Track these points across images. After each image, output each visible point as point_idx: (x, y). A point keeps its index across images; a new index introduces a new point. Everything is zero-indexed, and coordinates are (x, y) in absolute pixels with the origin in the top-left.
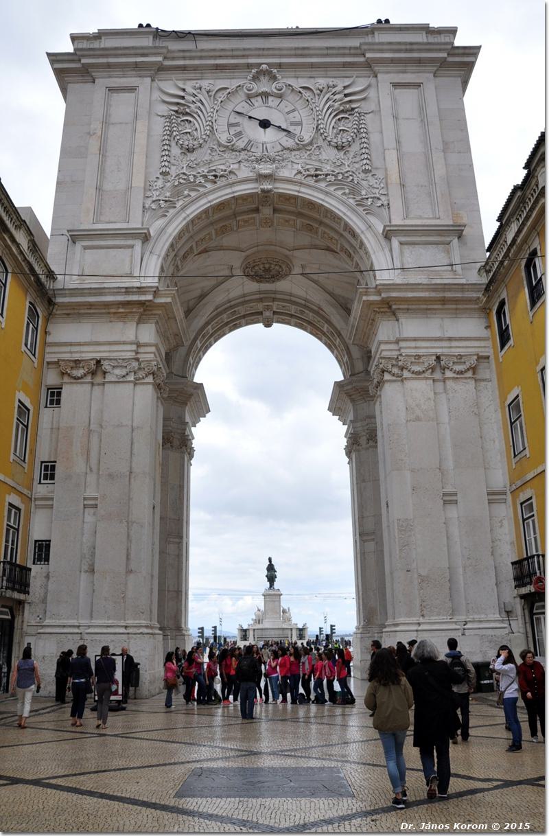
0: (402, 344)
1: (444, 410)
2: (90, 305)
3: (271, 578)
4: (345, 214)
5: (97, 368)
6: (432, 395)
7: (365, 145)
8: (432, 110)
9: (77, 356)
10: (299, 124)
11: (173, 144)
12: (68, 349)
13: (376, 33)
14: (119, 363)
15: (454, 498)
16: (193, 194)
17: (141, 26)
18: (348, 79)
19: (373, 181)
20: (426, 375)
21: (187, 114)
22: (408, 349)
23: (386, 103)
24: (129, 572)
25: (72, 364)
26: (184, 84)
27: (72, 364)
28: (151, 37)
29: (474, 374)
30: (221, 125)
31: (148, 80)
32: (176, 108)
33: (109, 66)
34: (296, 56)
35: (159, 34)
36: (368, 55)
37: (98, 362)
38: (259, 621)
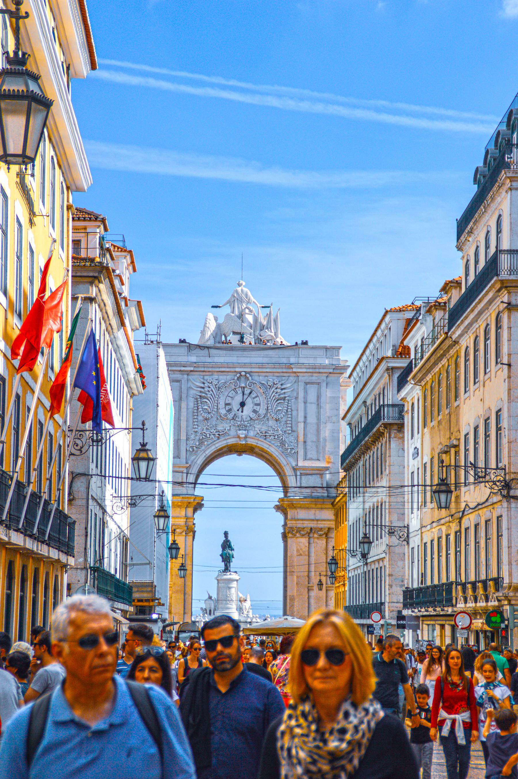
0: (298, 522)
1: (313, 550)
3: (227, 559)
6: (307, 545)
7: (289, 419)
10: (259, 405)
13: (300, 349)
17: (180, 340)
18: (283, 378)
19: (292, 439)
20: (306, 536)
22: (300, 524)
23: (301, 395)
28: (186, 348)
29: (326, 536)
30: (222, 405)
31: (186, 376)
34: (259, 368)
35: (191, 347)
36: (294, 370)
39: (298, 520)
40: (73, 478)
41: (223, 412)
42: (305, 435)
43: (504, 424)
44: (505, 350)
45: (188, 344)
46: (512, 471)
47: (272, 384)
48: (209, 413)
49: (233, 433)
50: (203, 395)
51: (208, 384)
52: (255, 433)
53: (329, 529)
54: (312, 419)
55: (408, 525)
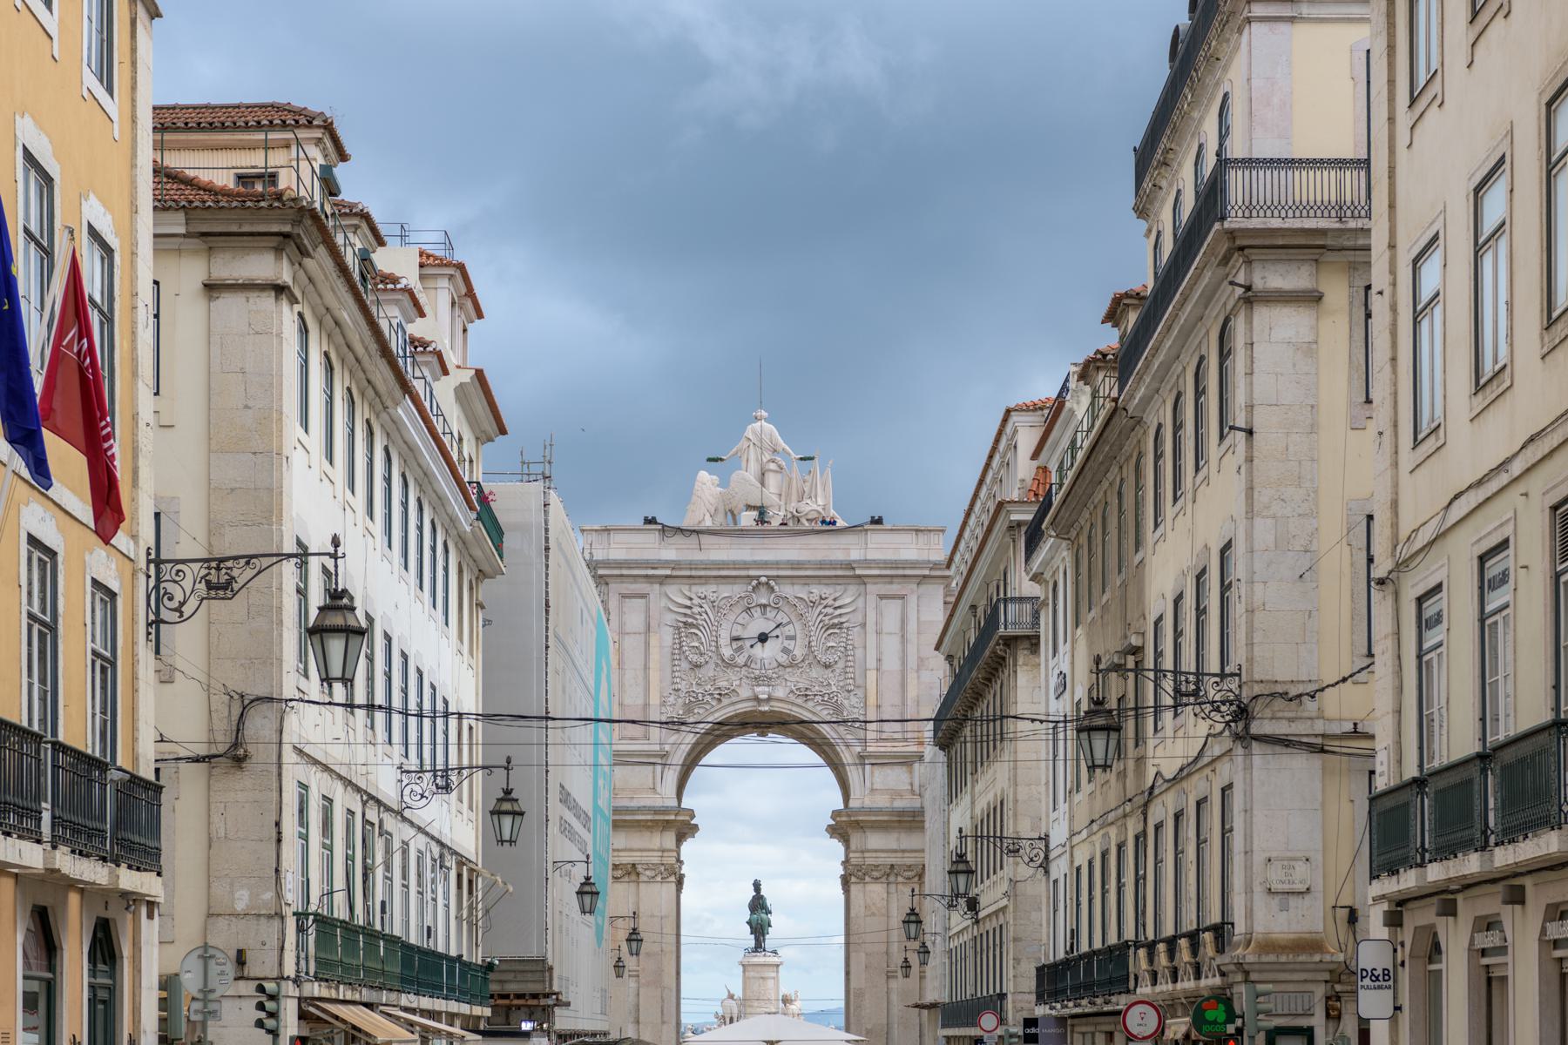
0: (866, 855)
2: (625, 821)
3: (759, 930)
7: (850, 664)
8: (912, 626)
10: (793, 638)
11: (683, 658)
13: (869, 533)
14: (648, 867)
19: (854, 700)
20: (883, 880)
21: (692, 625)
24: (663, 1022)
26: (690, 591)
30: (724, 640)
31: (657, 587)
32: (684, 620)
33: (622, 576)
36: (858, 572)
37: (634, 865)
39: (869, 851)
40: (244, 708)
41: (727, 652)
43: (1239, 570)
44: (1239, 398)
45: (660, 527)
46: (1257, 677)
47: (818, 598)
48: (701, 654)
49: (745, 692)
50: (690, 620)
51: (700, 601)
52: (788, 690)
54: (892, 663)
55: (1047, 836)
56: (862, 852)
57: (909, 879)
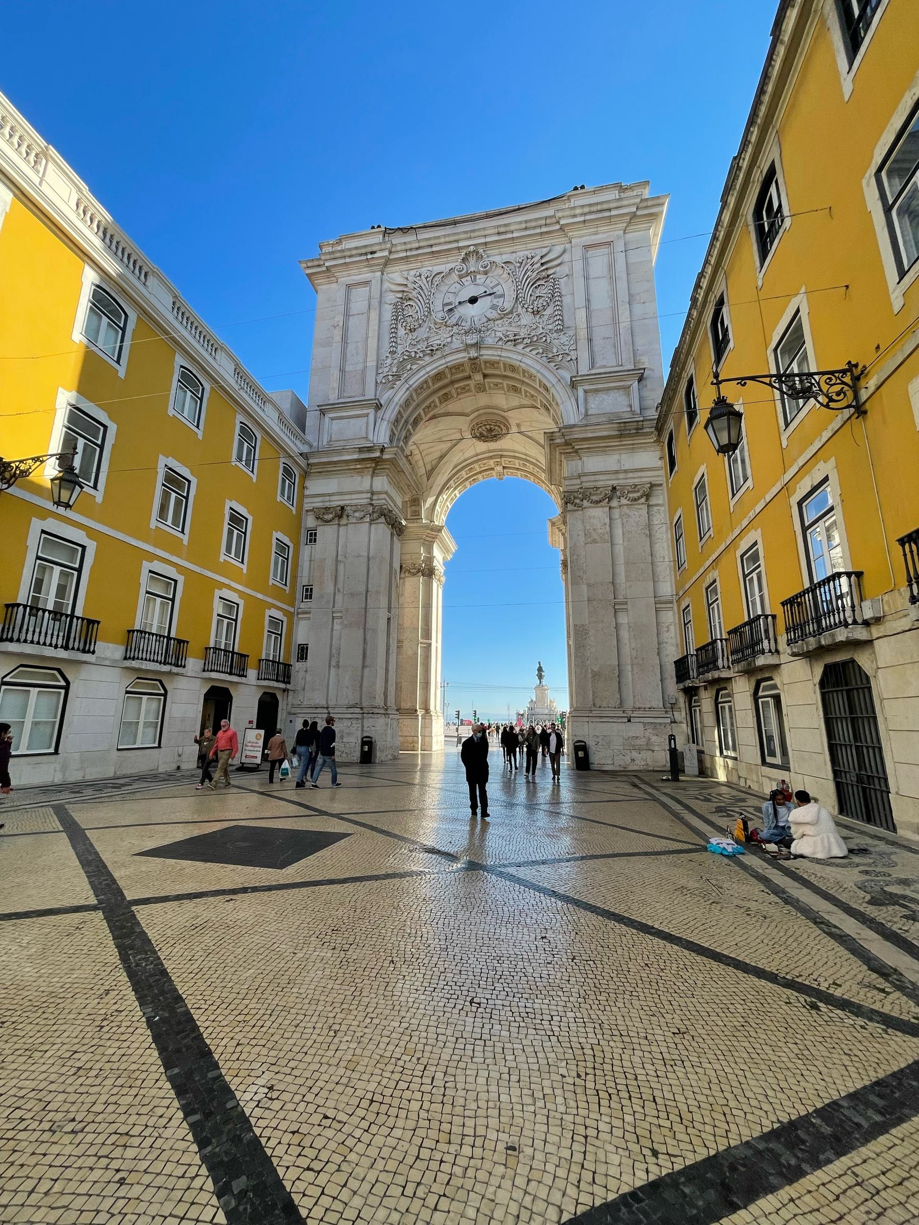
0: (584, 479)
1: (618, 531)
3: (540, 677)
4: (538, 371)
5: (341, 512)
6: (607, 521)
9: (327, 504)
10: (503, 296)
12: (321, 499)
15: (625, 607)
16: (414, 367)
19: (564, 339)
20: (603, 503)
23: (578, 266)
25: (323, 511)
27: (323, 511)
29: (647, 500)
30: (438, 305)
34: (499, 233)
36: (562, 222)
37: (343, 508)
38: (531, 709)
39: (585, 475)
42: (589, 328)
49: (457, 344)
53: (652, 486)
56: (579, 476)
57: (635, 500)
